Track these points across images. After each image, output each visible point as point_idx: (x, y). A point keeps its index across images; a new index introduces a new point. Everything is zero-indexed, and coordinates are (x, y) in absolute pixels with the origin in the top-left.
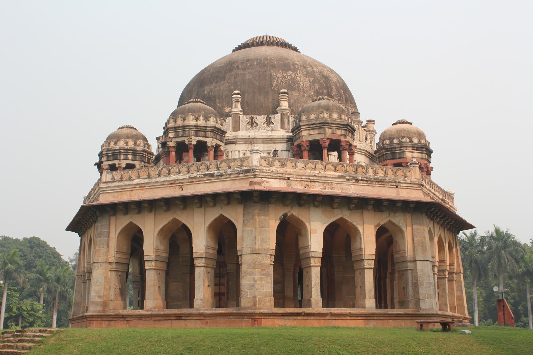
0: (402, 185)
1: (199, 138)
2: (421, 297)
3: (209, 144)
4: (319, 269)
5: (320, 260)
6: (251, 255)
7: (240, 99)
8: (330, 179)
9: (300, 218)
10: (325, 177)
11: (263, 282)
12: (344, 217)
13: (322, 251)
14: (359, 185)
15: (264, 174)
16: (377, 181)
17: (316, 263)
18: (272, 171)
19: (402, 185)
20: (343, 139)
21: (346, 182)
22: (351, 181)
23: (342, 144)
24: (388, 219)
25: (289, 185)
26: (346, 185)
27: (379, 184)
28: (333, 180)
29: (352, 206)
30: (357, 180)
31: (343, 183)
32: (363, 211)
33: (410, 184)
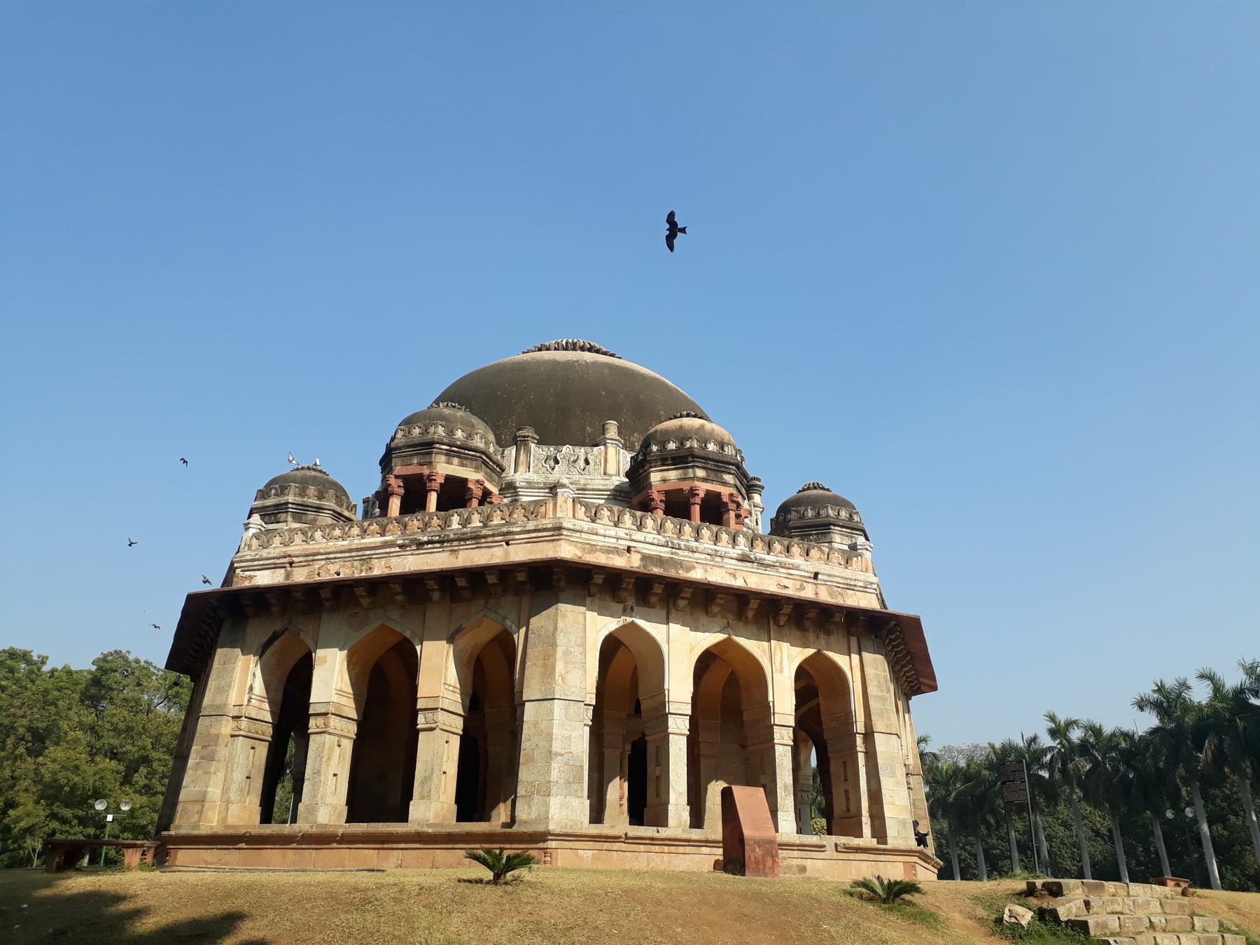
0: (517, 537)
8: (368, 552)
10: (357, 550)
16: (462, 539)
17: (318, 727)
21: (399, 552)
22: (408, 549)
26: (397, 558)
27: (468, 543)
28: (373, 552)
30: (420, 545)
31: (391, 555)
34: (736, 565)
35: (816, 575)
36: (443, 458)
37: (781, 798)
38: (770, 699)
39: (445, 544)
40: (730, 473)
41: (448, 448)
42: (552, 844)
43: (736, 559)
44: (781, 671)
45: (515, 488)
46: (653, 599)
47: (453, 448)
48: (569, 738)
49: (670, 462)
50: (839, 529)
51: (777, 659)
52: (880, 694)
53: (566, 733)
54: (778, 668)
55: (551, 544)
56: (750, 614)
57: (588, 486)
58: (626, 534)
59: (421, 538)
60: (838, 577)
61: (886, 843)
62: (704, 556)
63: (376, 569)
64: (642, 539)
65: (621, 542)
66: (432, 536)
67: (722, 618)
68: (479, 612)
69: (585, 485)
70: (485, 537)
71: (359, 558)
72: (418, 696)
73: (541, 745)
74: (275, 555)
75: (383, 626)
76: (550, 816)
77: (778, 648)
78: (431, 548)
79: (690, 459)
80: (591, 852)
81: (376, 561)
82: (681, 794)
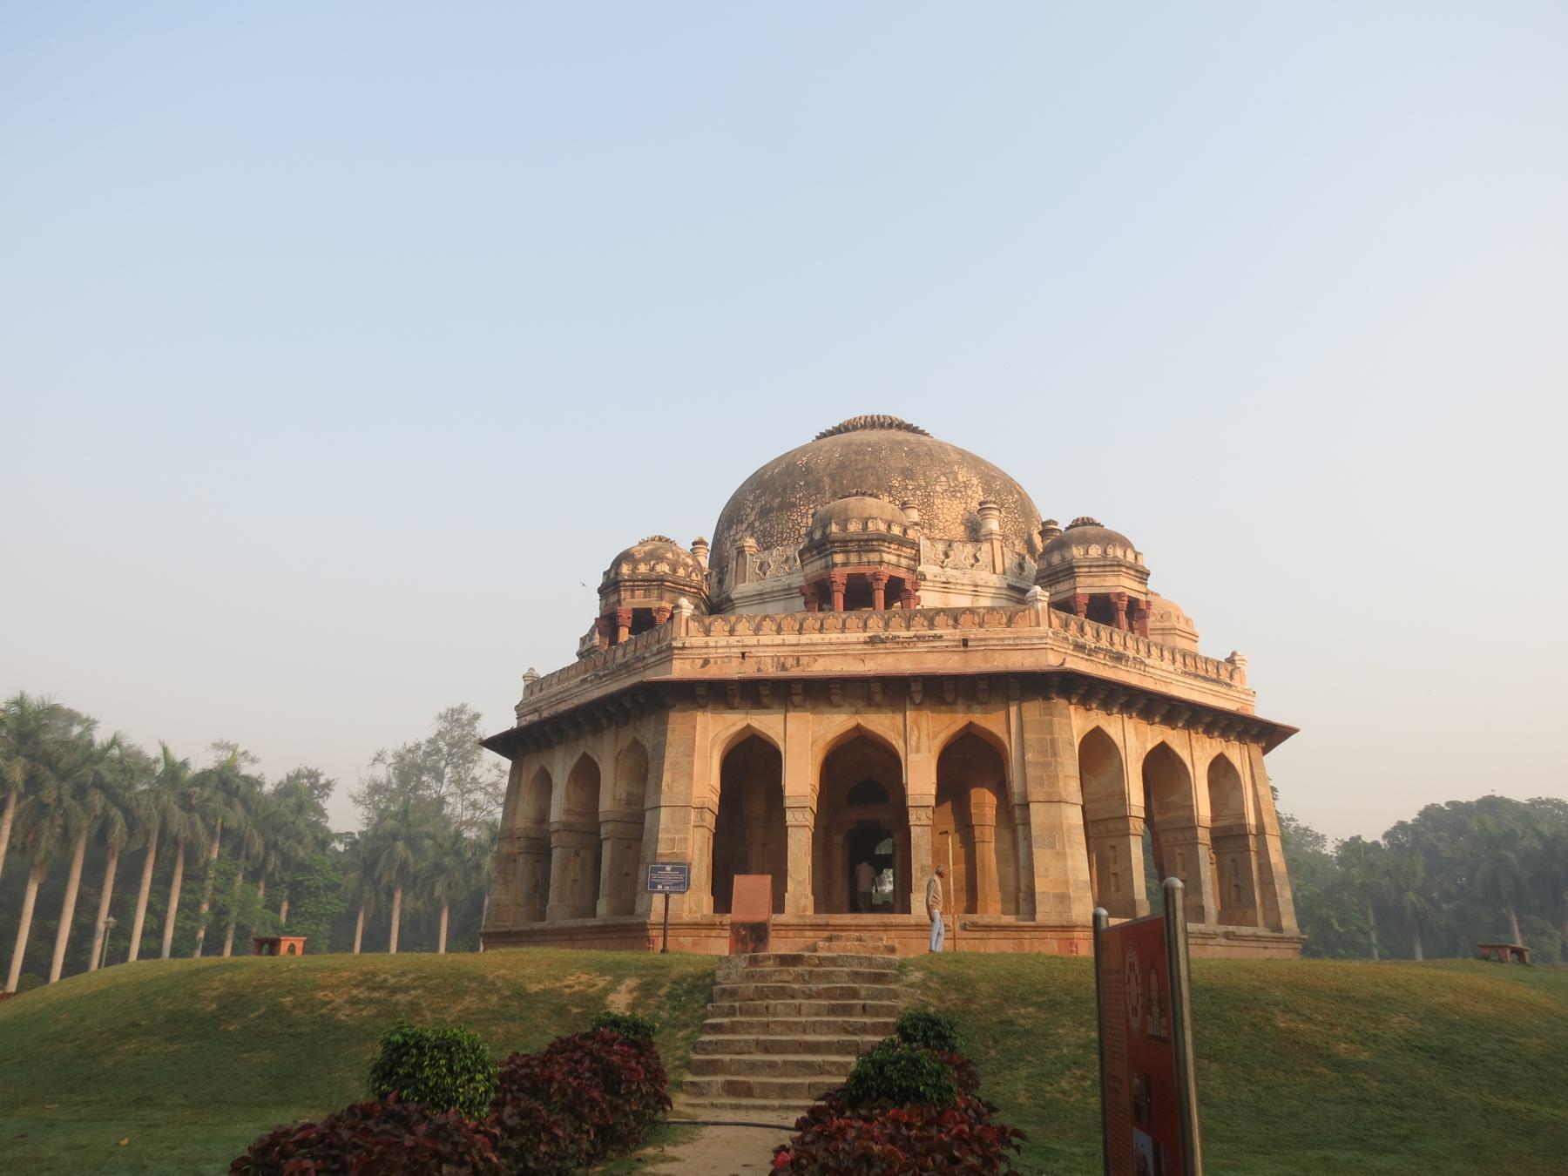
0: (650, 661)
19: (650, 661)
34: (865, 650)
35: (965, 642)
36: (629, 593)
37: (916, 878)
38: (904, 782)
40: (877, 551)
41: (631, 584)
43: (865, 643)
44: (918, 751)
45: (731, 600)
46: (765, 701)
47: (636, 583)
48: (673, 840)
49: (815, 552)
50: (1087, 570)
51: (913, 740)
52: (1041, 760)
53: (671, 836)
54: (914, 749)
56: (878, 698)
57: (793, 586)
58: (739, 641)
60: (992, 639)
61: (1034, 920)
62: (825, 648)
64: (756, 643)
65: (733, 650)
67: (850, 707)
69: (789, 585)
72: (600, 811)
75: (585, 754)
76: (653, 909)
77: (915, 728)
80: (691, 939)
82: (799, 882)
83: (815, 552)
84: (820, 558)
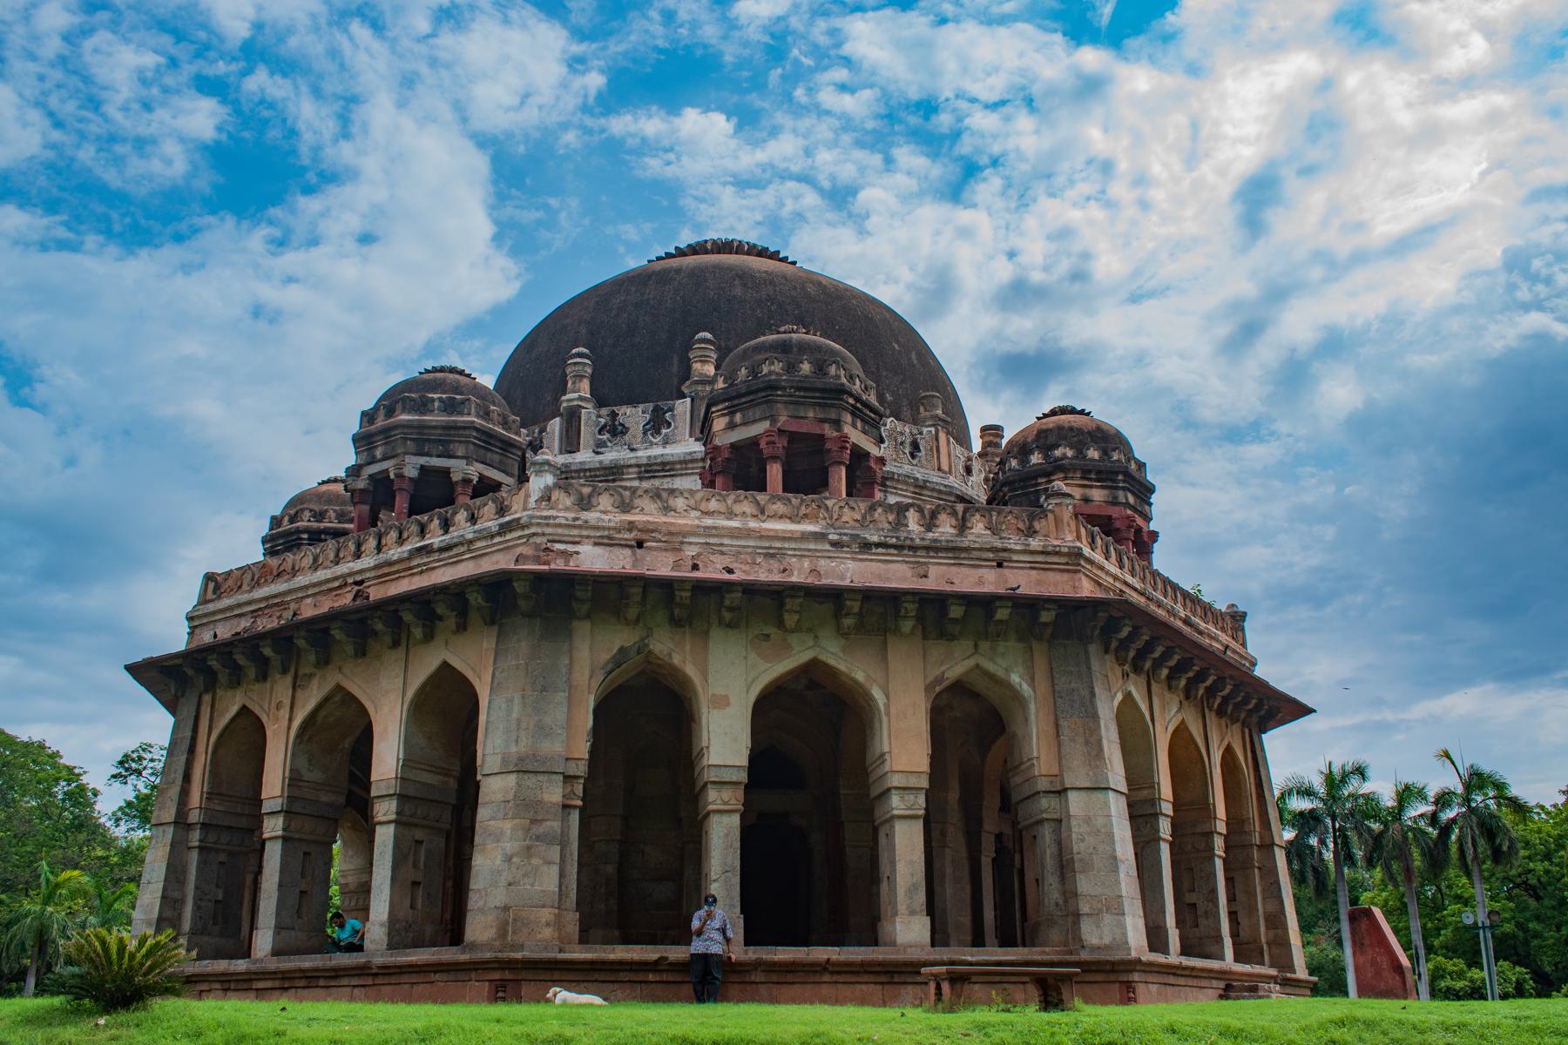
0: (1015, 558)
1: (428, 459)
2: (1085, 908)
3: (456, 477)
4: (735, 820)
5: (740, 793)
6: (504, 776)
7: (589, 370)
8: (778, 545)
9: (676, 660)
11: (536, 861)
12: (823, 658)
13: (745, 762)
14: (871, 560)
15: (560, 531)
16: (933, 548)
18: (586, 522)
19: (1015, 558)
20: (828, 431)
21: (829, 551)
22: (845, 549)
23: (828, 446)
24: (971, 663)
25: (636, 562)
26: (828, 561)
27: (940, 555)
29: (848, 622)
30: (866, 546)
32: (885, 642)
33: (1042, 553)
39: (906, 552)
42: (1136, 977)
55: (1066, 576)
59: (867, 536)
63: (796, 573)
66: (885, 537)
68: (969, 657)
70: (967, 549)
71: (764, 551)
73: (1101, 848)
74: (612, 524)
78: (883, 554)
79: (1120, 477)
81: (794, 560)
83: (1093, 476)
84: (1102, 487)
